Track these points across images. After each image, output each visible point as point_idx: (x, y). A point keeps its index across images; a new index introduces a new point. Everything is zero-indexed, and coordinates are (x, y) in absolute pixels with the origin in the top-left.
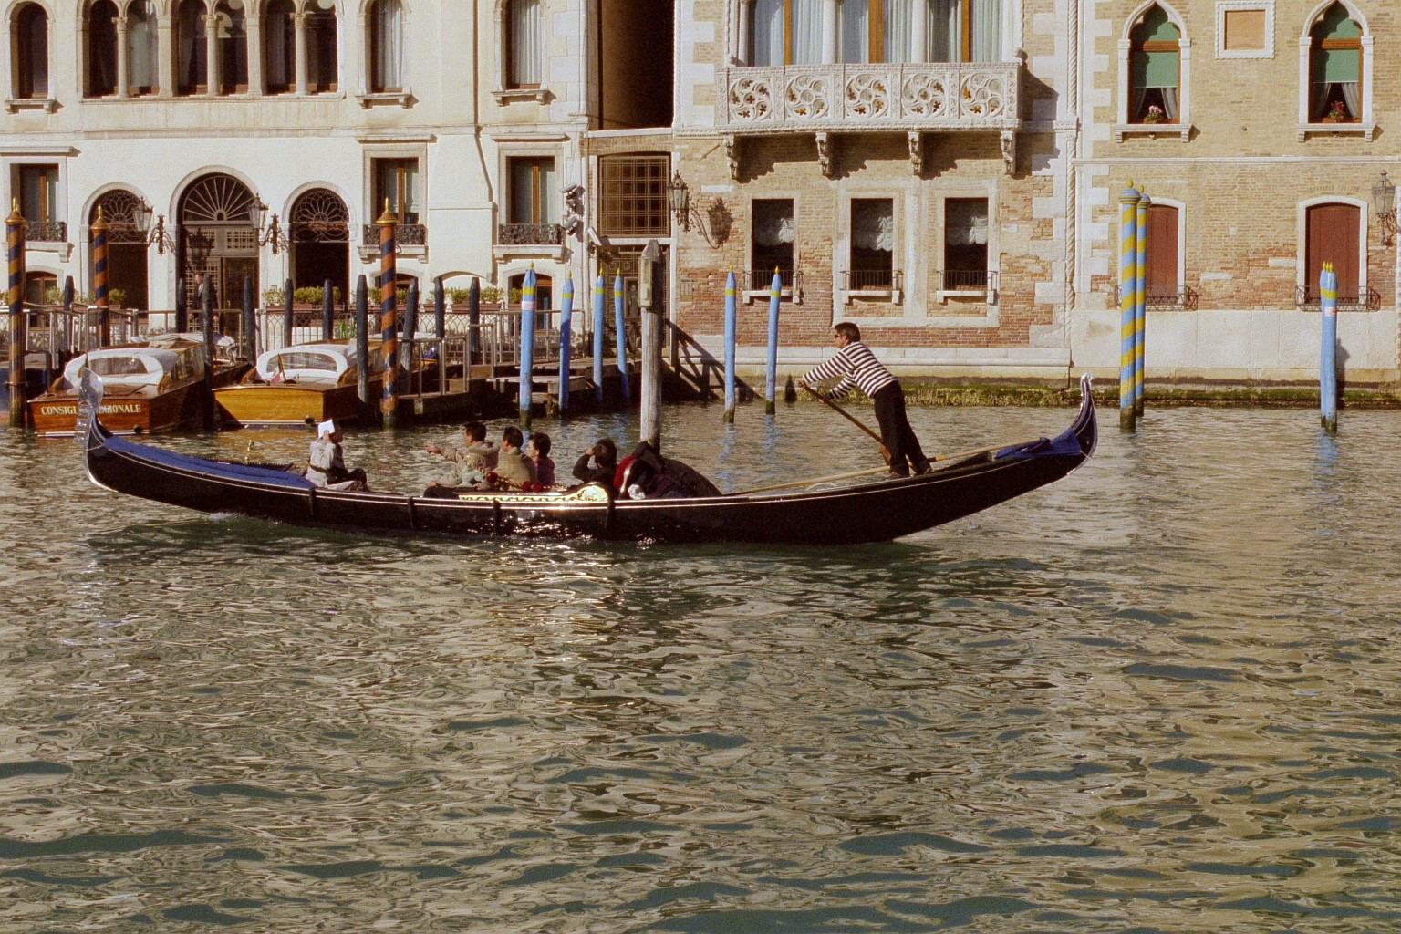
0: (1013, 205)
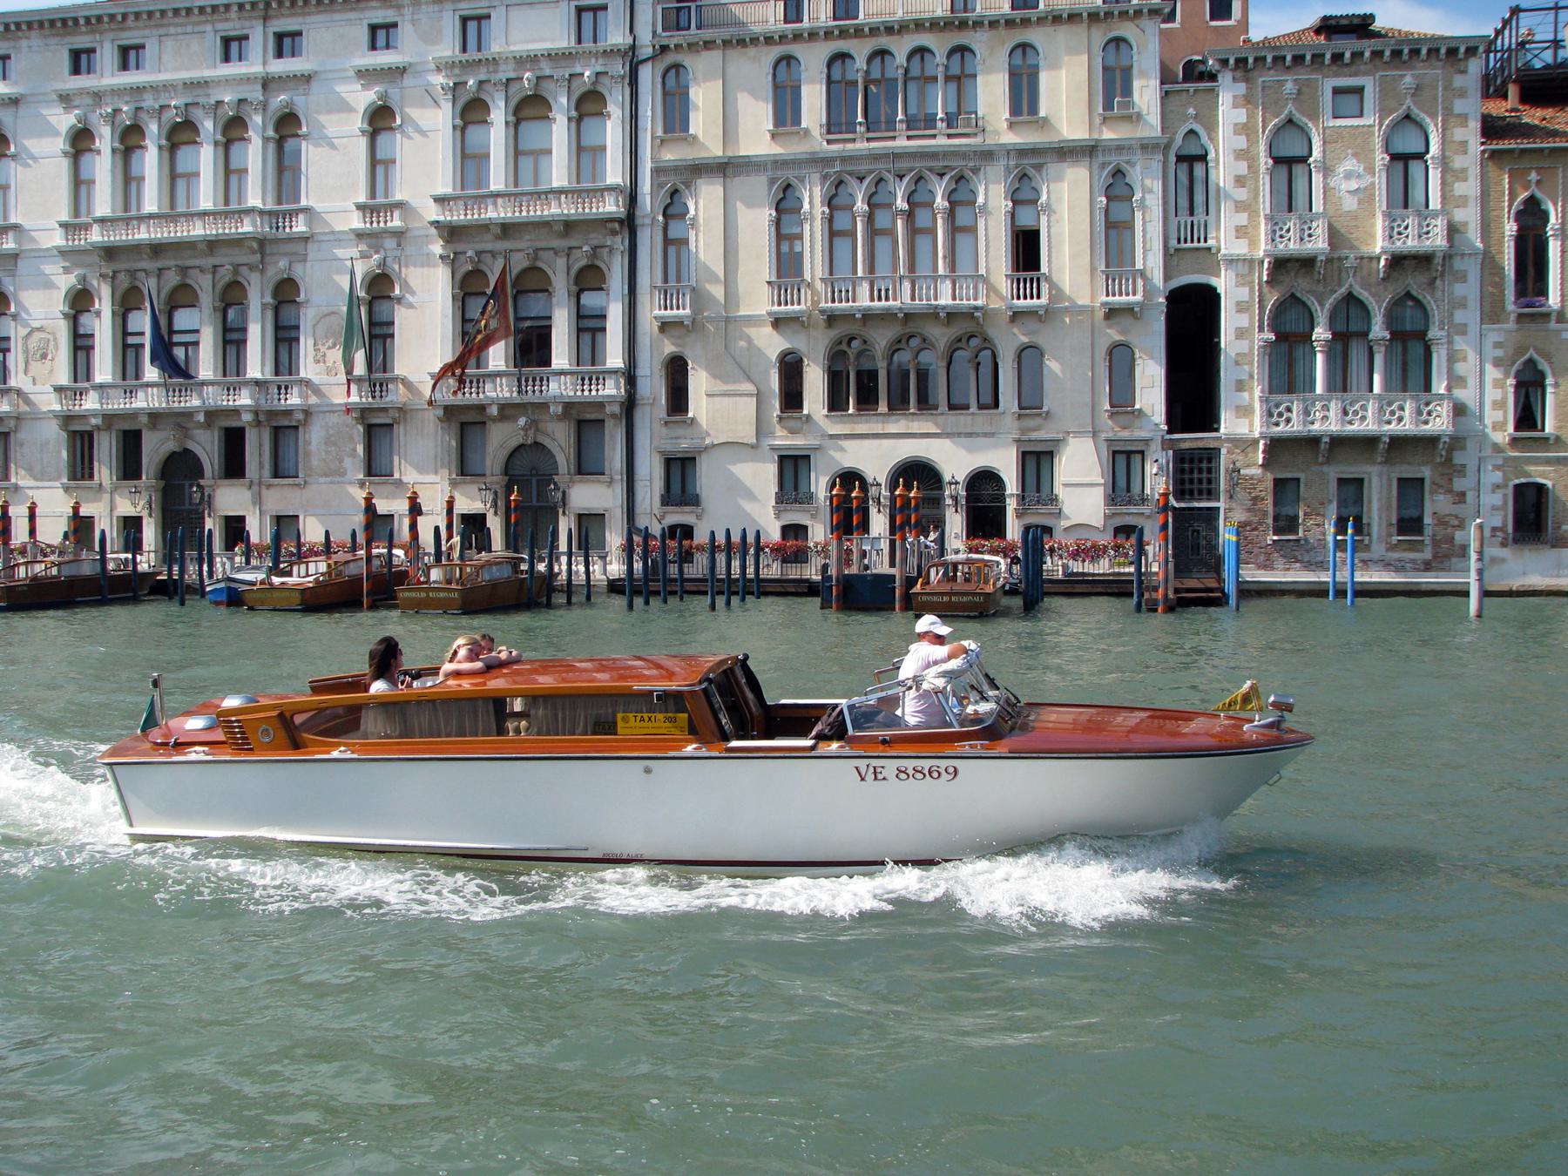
0: (1443, 483)
